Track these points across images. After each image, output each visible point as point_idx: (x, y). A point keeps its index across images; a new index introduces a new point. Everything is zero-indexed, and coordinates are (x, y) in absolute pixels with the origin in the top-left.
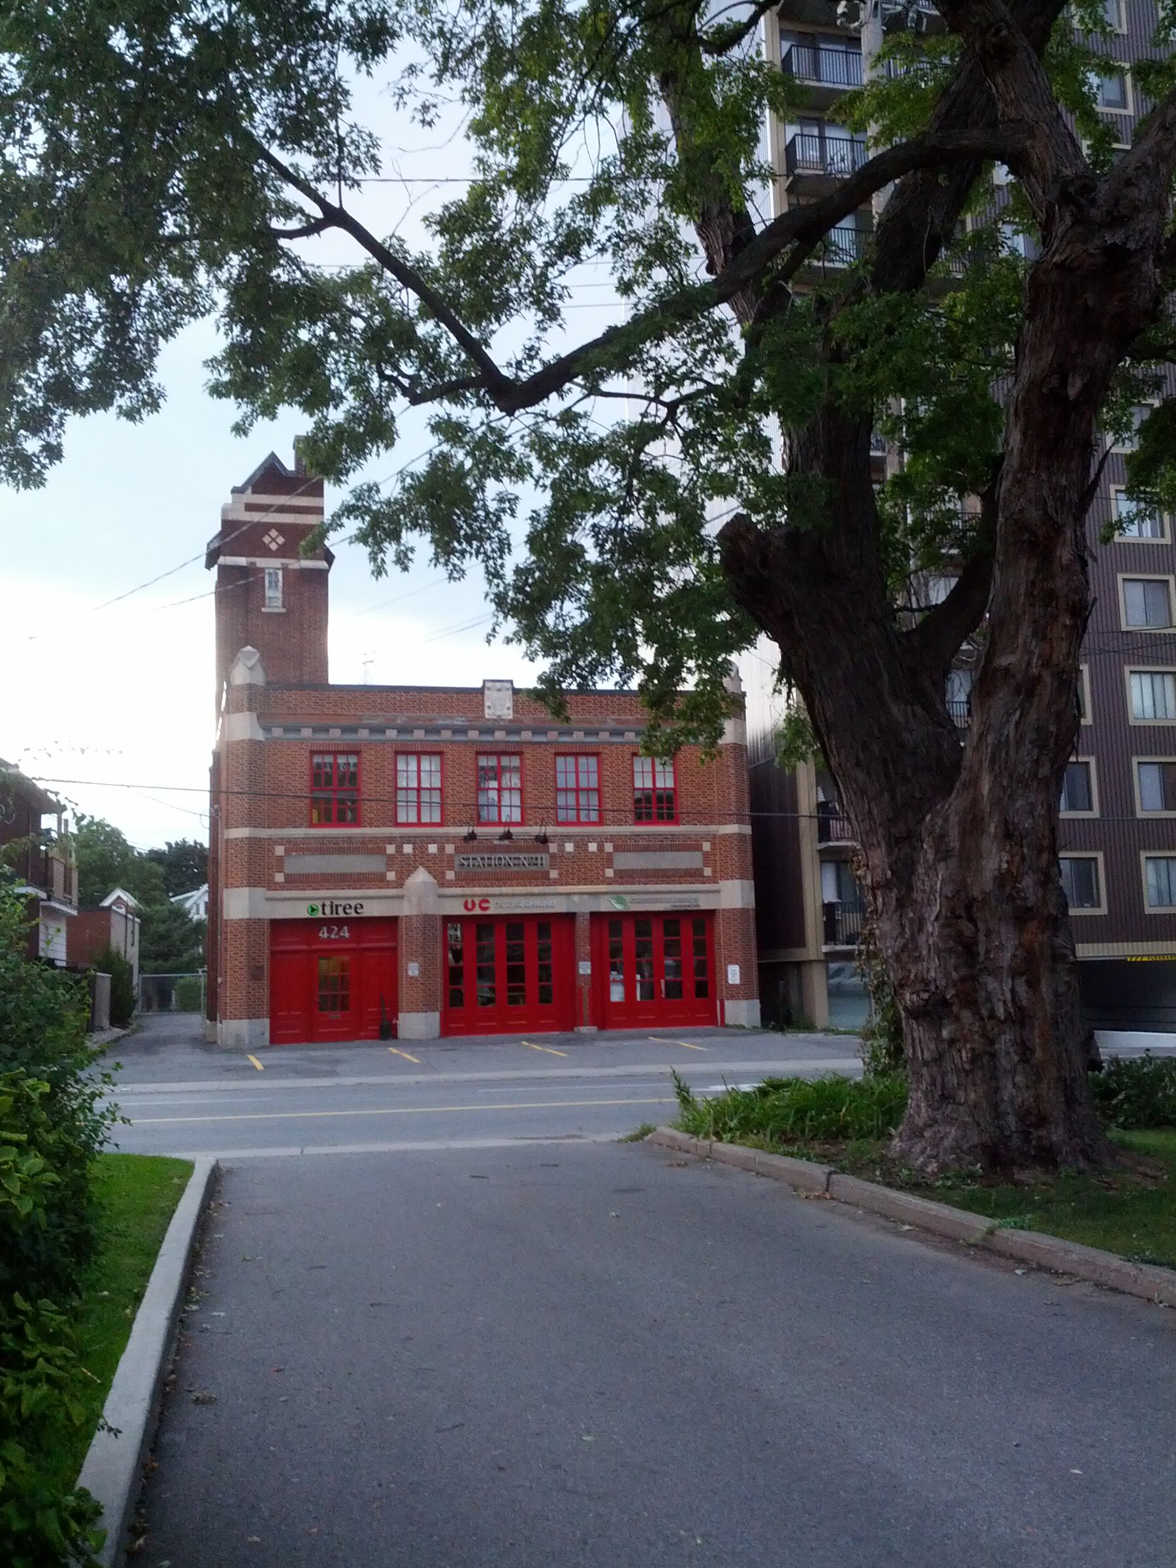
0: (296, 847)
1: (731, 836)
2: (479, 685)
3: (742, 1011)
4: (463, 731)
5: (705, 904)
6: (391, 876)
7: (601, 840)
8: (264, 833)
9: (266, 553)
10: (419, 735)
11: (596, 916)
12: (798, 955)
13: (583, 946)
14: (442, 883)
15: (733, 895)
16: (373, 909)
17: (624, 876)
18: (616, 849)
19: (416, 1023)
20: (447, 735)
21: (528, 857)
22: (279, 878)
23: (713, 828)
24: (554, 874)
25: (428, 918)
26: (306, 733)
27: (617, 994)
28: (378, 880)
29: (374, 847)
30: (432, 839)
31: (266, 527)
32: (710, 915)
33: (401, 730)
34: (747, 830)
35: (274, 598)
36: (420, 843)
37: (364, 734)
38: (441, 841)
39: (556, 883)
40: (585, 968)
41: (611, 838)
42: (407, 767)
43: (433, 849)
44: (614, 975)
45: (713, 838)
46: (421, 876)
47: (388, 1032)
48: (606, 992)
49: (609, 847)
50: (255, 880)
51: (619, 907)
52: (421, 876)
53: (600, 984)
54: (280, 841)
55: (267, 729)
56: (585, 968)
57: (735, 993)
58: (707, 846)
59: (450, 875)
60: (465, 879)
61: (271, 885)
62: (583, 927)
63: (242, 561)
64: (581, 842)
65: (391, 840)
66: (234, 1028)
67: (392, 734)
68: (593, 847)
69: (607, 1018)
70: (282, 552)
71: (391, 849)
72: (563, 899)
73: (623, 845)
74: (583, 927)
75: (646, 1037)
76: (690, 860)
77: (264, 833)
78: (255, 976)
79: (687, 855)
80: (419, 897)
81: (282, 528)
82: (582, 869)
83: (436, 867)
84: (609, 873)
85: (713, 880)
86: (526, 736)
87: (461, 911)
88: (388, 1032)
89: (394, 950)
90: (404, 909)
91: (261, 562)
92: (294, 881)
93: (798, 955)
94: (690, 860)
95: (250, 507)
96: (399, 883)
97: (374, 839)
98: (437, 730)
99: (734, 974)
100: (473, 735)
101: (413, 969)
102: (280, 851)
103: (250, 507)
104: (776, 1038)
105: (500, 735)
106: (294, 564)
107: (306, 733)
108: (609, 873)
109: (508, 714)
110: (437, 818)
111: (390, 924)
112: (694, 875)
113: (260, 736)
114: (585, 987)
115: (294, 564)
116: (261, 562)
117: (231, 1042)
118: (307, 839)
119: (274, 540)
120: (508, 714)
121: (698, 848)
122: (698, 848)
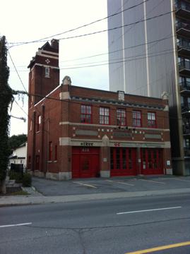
0: (78, 128)
2: (116, 91)
3: (170, 171)
4: (114, 102)
5: (162, 146)
6: (99, 136)
7: (142, 131)
8: (71, 124)
9: (46, 64)
10: (105, 102)
11: (141, 148)
12: (179, 159)
14: (110, 139)
15: (167, 145)
16: (95, 145)
17: (147, 140)
18: (146, 133)
19: (105, 173)
20: (111, 103)
21: (128, 134)
22: (74, 135)
25: (107, 147)
26: (80, 99)
27: (144, 167)
28: (96, 137)
29: (95, 129)
30: (108, 128)
31: (46, 58)
32: (162, 149)
35: (47, 75)
36: (105, 128)
37: (93, 101)
38: (110, 128)
40: (140, 161)
41: (144, 130)
42: (101, 110)
43: (108, 130)
45: (163, 132)
46: (106, 137)
47: (98, 176)
48: (142, 167)
50: (70, 136)
51: (146, 147)
52: (106, 137)
54: (75, 126)
55: (71, 97)
57: (168, 167)
60: (115, 138)
61: (72, 137)
62: (139, 151)
63: (41, 65)
65: (99, 128)
66: (61, 174)
67: (99, 101)
69: (143, 172)
70: (49, 64)
71: (99, 130)
74: (139, 151)
75: (157, 177)
76: (158, 137)
77: (71, 124)
78: (69, 161)
80: (105, 142)
81: (50, 59)
82: (139, 137)
83: (108, 134)
86: (127, 105)
88: (98, 176)
89: (98, 155)
90: (102, 145)
91: (45, 66)
92: (78, 136)
93: (179, 159)
94: (158, 137)
95: (42, 53)
97: (96, 127)
98: (109, 102)
99: (169, 163)
100: (117, 104)
101: (105, 160)
102: (74, 128)
103: (42, 53)
104: (177, 179)
105: (122, 104)
106: (52, 67)
107: (80, 99)
109: (123, 100)
110: (108, 123)
111: (99, 148)
112: (159, 140)
114: (140, 165)
115: (52, 67)
116: (45, 66)
117: (63, 178)
118: (80, 126)
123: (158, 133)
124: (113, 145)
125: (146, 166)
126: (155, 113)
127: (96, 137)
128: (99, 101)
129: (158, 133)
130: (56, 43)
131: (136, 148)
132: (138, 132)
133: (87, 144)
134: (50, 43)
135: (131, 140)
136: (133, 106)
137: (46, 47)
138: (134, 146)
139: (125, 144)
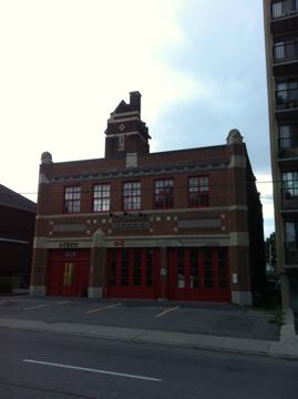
1: (233, 211)
5: (222, 243)
7: (172, 215)
9: (120, 132)
13: (164, 262)
14: (107, 234)
16: (81, 245)
17: (182, 231)
23: (226, 208)
24: (151, 230)
27: (181, 285)
28: (83, 234)
31: (119, 124)
32: (226, 248)
33: (94, 176)
34: (245, 208)
39: (152, 234)
40: (163, 272)
41: (177, 214)
43: (104, 221)
44: (180, 276)
45: (226, 212)
49: (176, 218)
51: (179, 245)
52: (99, 232)
53: (171, 279)
54: (52, 220)
55: (49, 179)
56: (163, 272)
58: (223, 216)
59: (110, 231)
60: (116, 233)
64: (163, 217)
65: (89, 218)
67: (91, 177)
68: (169, 218)
69: (173, 295)
70: (125, 131)
71: (89, 222)
72: (154, 241)
73: (182, 217)
79: (214, 221)
80: (97, 240)
82: (163, 228)
83: (105, 228)
84: (176, 229)
85: (227, 232)
86: (141, 173)
87: (113, 246)
92: (56, 234)
95: (115, 118)
96: (91, 236)
103: (115, 118)
106: (128, 134)
107: (62, 180)
108: (176, 229)
109: (135, 165)
112: (216, 230)
113: (47, 182)
115: (128, 134)
119: (122, 128)
120: (135, 165)
121: (218, 218)
122: (218, 218)
123: (215, 216)
124: (111, 245)
125: (187, 283)
126: (65, 187)
127: (84, 234)
128: (91, 177)
129: (215, 216)
130: (136, 97)
131: (157, 249)
132: (164, 218)
133: (68, 244)
134: (128, 102)
135: (149, 234)
136: (152, 172)
137: (122, 107)
138: (152, 244)
139: (133, 242)
